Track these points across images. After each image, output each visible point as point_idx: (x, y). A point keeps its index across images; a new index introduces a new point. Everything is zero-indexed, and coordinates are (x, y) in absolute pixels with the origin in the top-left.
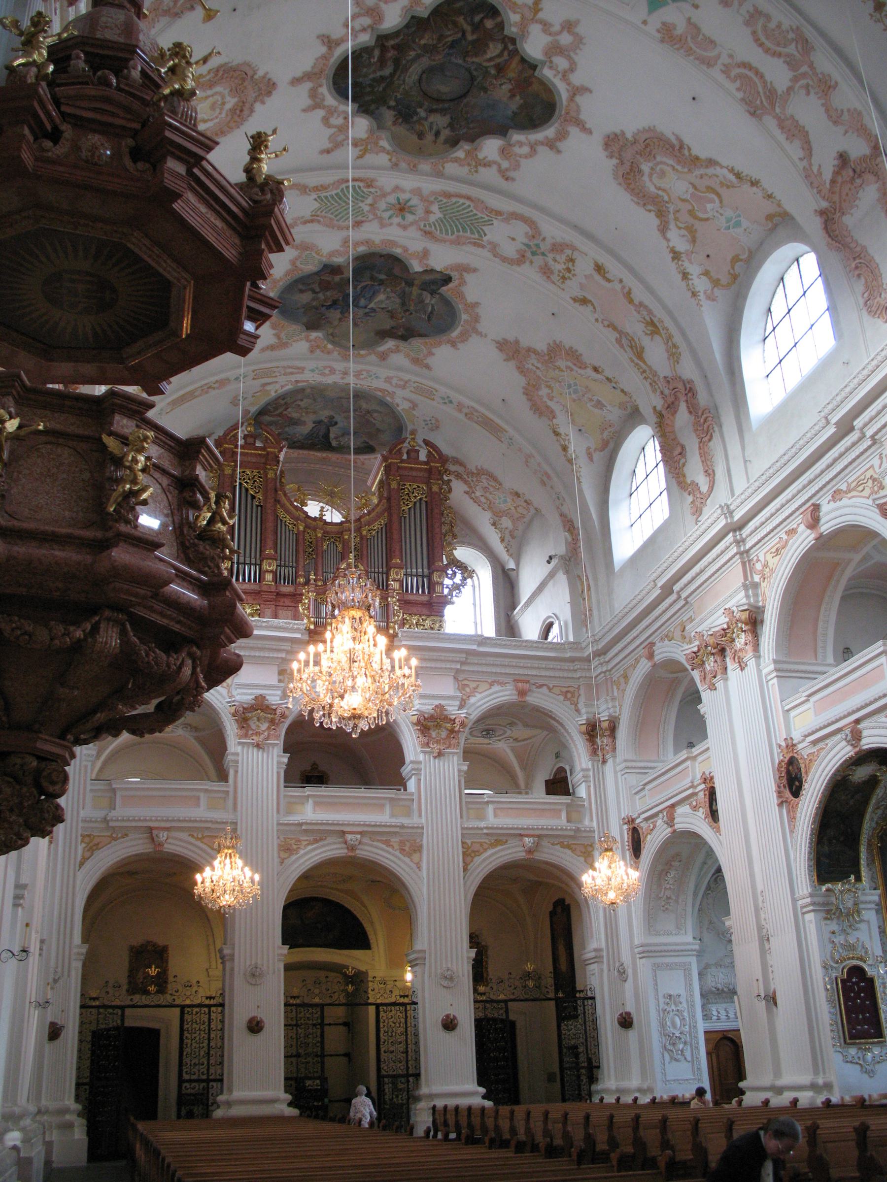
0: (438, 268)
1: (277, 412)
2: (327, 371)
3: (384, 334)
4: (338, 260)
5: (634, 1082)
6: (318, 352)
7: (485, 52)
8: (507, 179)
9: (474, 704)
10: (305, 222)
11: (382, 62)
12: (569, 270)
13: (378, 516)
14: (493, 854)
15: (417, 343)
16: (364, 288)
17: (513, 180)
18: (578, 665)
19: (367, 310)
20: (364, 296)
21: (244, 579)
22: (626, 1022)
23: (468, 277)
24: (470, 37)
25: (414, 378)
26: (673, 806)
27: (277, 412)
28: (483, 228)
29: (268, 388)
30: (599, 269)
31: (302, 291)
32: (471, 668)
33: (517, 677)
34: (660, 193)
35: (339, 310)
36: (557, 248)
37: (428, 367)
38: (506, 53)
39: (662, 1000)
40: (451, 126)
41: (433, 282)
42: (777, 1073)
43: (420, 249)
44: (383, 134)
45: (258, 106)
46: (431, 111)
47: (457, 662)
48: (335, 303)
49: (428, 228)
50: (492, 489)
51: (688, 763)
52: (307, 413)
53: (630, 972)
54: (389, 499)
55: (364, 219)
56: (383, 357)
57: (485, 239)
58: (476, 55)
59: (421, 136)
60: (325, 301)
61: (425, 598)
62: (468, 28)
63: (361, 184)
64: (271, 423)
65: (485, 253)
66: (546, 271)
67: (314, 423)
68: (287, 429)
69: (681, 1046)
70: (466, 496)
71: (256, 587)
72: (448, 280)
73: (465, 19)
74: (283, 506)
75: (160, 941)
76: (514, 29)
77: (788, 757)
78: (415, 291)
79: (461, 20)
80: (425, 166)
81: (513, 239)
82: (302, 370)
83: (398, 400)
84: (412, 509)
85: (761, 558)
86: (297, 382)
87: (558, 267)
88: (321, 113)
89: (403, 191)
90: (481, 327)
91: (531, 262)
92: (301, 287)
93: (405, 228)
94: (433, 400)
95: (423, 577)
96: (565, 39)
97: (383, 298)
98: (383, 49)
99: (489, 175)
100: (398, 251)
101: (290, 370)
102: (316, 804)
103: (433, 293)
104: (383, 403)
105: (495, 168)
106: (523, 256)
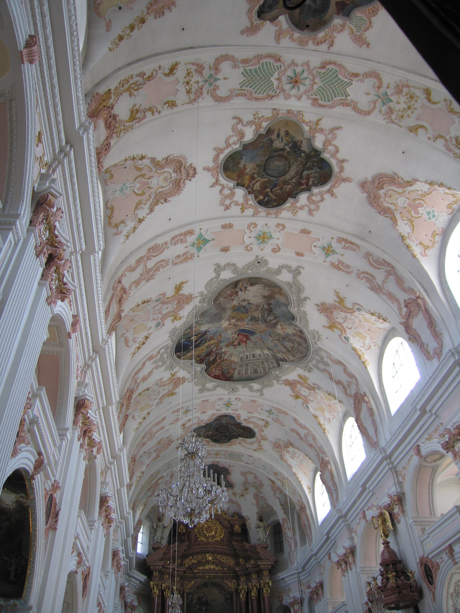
7: (261, 184)
11: (308, 178)
24: (268, 190)
28: (245, 79)
34: (162, 171)
38: (251, 186)
40: (272, 141)
44: (307, 135)
45: (370, 179)
46: (283, 150)
55: (319, 71)
57: (242, 70)
58: (264, 182)
59: (287, 133)
62: (270, 194)
73: (272, 198)
76: (250, 197)
79: (274, 197)
88: (340, 156)
93: (293, 63)
96: (228, 202)
98: (307, 184)
99: (247, 117)
100: (297, 35)
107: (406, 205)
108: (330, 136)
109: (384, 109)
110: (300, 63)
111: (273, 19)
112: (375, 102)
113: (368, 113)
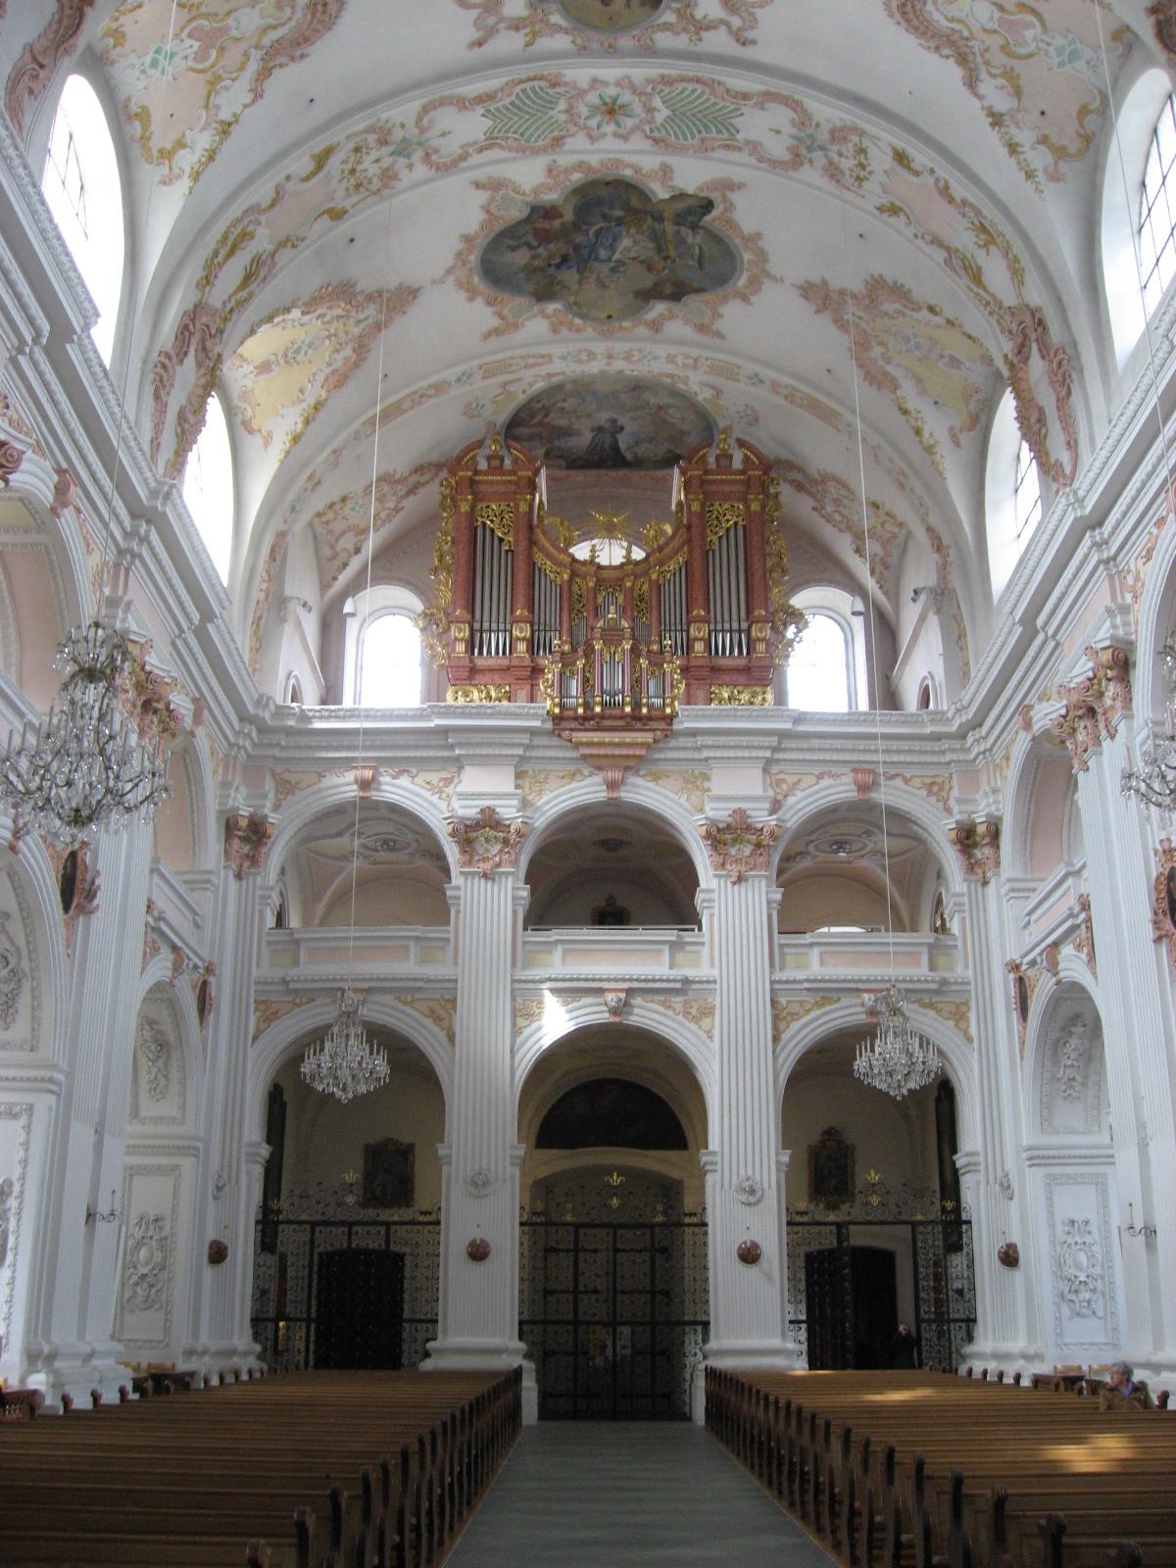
0: (690, 191)
1: (535, 421)
2: (584, 357)
3: (646, 296)
4: (551, 197)
5: (1018, 1345)
6: (564, 332)
8: (744, 44)
9: (792, 807)
10: (480, 150)
12: (862, 166)
13: (676, 552)
14: (817, 1018)
15: (693, 301)
16: (598, 233)
17: (754, 42)
18: (945, 745)
19: (612, 264)
20: (602, 245)
21: (489, 652)
22: (1010, 1258)
23: (736, 197)
25: (705, 354)
26: (1056, 945)
27: (535, 421)
28: (734, 121)
29: (512, 388)
30: (901, 157)
31: (513, 249)
32: (787, 756)
33: (856, 766)
34: (955, 25)
35: (574, 270)
36: (839, 135)
37: (719, 335)
39: (1060, 1229)
41: (689, 211)
42: (1159, 1344)
43: (657, 166)
47: (767, 748)
48: (565, 259)
49: (656, 134)
50: (845, 501)
51: (1070, 881)
52: (578, 418)
53: (1015, 1185)
54: (689, 527)
56: (656, 326)
60: (550, 257)
61: (742, 662)
63: (543, 83)
64: (531, 438)
65: (743, 157)
66: (833, 172)
67: (592, 430)
68: (557, 443)
69: (1087, 1296)
70: (815, 514)
71: (505, 662)
72: (708, 206)
74: (542, 549)
75: (405, 1138)
77: (1168, 867)
78: (669, 228)
80: (625, 42)
81: (778, 132)
82: (549, 358)
83: (695, 388)
84: (724, 540)
85: (1132, 567)
86: (549, 375)
87: (847, 164)
89: (606, 84)
90: (775, 266)
91: (811, 162)
92: (511, 242)
93: (625, 138)
94: (738, 380)
95: (740, 631)
97: (629, 244)
100: (628, 173)
101: (531, 361)
102: (565, 952)
103: (694, 227)
104: (675, 394)
105: (723, 29)
106: (798, 155)
107: (230, 21)
108: (491, 21)
109: (398, 135)
110: (610, 138)
111: (681, 196)
112: (423, 130)
113: (426, 109)
